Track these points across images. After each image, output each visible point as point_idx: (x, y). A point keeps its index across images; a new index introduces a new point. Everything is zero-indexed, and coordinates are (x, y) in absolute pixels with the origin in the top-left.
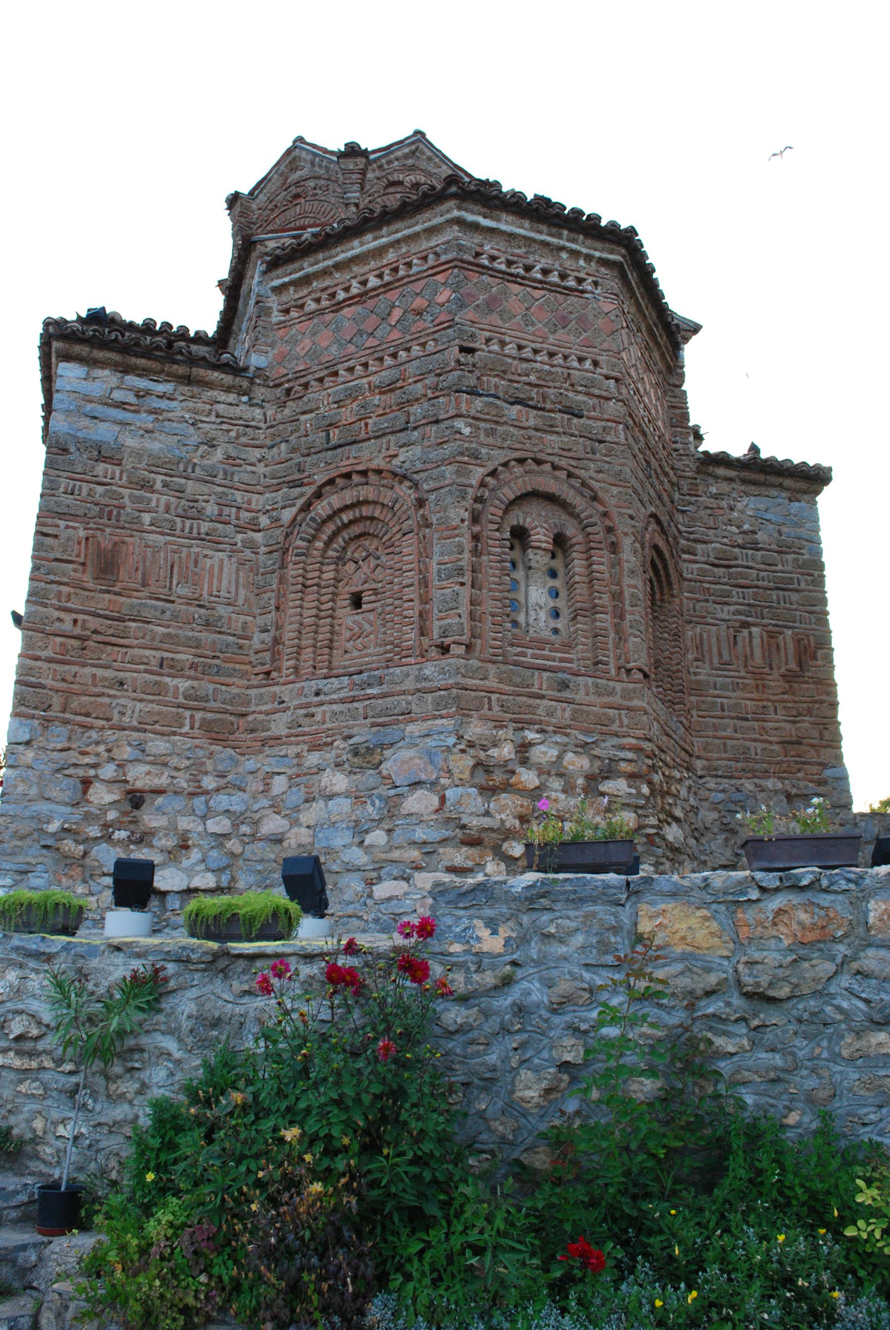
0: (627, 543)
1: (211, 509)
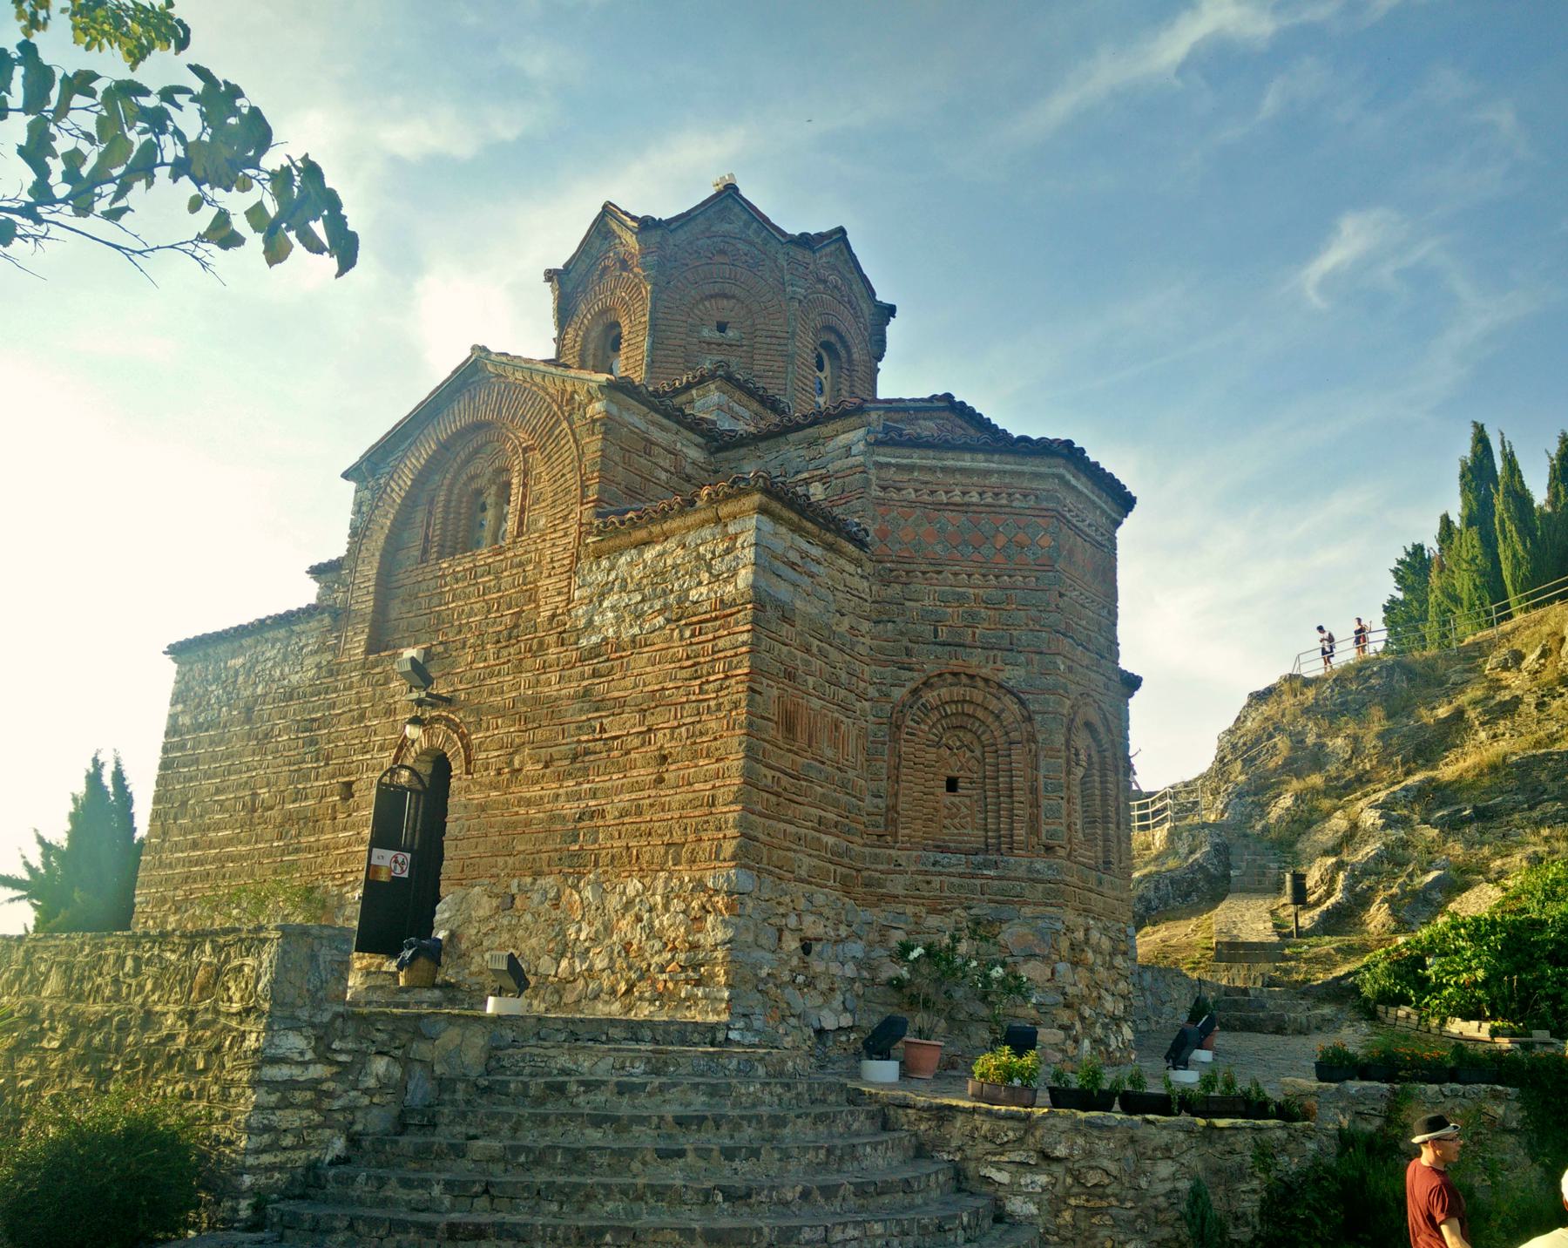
1: (844, 676)
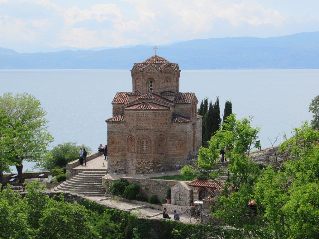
0: (152, 142)
